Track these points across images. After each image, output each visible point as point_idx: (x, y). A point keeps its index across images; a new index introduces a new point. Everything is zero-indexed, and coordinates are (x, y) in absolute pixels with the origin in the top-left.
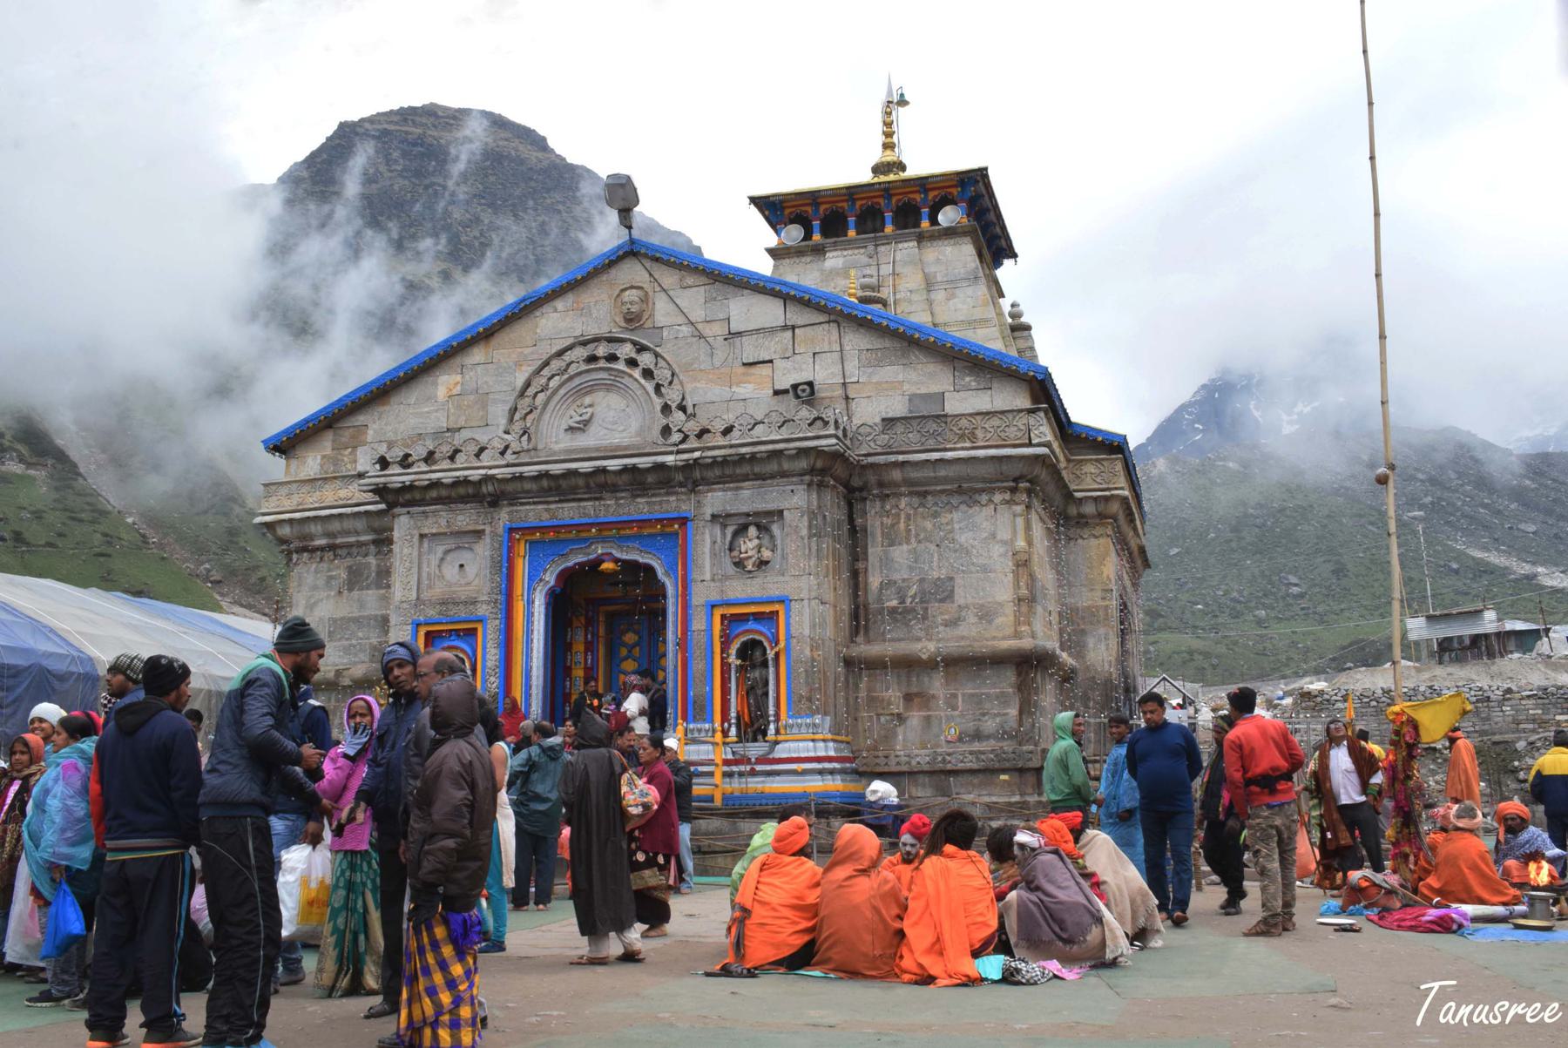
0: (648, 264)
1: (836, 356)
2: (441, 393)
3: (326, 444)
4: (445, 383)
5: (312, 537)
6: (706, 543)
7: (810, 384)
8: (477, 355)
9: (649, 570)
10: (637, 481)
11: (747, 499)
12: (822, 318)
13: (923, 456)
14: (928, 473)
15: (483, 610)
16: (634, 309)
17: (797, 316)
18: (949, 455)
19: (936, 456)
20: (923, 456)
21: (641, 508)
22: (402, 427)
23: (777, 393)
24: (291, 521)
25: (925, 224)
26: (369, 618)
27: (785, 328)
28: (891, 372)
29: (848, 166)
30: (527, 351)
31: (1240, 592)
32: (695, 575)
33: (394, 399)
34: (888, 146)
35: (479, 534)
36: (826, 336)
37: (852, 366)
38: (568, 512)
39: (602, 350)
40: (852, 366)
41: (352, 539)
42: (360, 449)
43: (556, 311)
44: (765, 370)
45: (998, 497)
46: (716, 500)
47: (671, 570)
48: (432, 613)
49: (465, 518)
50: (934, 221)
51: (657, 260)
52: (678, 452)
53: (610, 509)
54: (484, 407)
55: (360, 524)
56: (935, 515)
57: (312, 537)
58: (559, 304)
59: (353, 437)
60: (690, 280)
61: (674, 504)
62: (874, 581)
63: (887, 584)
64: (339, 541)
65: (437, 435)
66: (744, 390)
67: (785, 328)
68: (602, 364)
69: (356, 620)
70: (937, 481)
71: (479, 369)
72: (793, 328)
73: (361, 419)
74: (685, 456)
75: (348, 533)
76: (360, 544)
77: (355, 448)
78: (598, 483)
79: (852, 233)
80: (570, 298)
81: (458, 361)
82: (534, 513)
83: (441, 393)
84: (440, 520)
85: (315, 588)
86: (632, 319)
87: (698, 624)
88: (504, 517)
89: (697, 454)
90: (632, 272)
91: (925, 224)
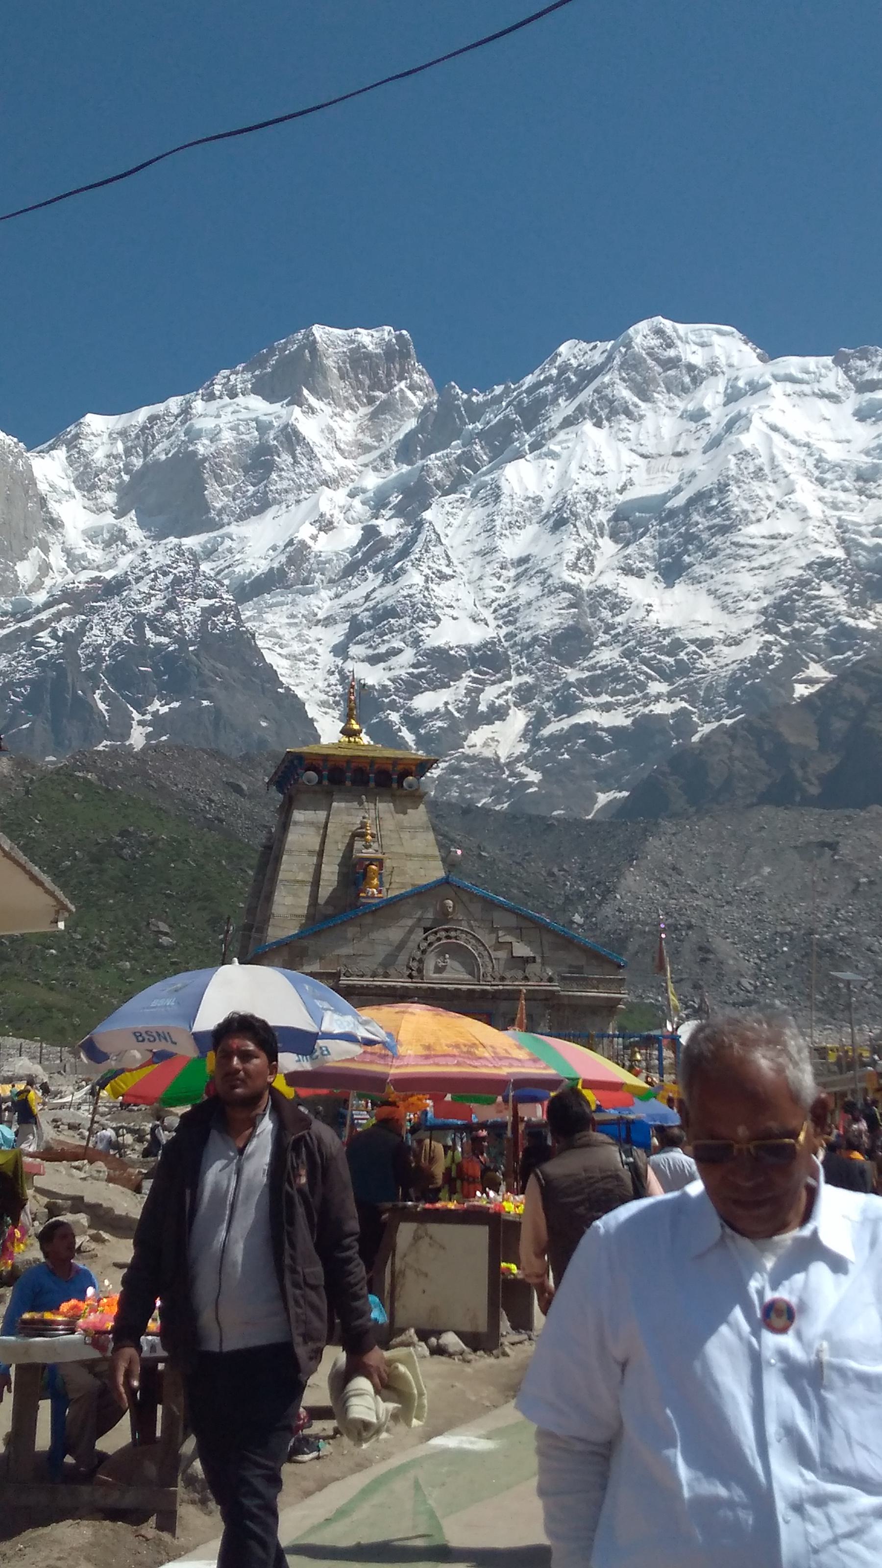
12: (532, 925)
13: (579, 994)
19: (584, 994)
20: (579, 994)
25: (395, 785)
27: (517, 928)
31: (101, 938)
43: (408, 903)
50: (400, 785)
52: (492, 985)
67: (517, 928)
72: (521, 929)
74: (495, 988)
79: (348, 783)
89: (501, 987)
91: (395, 785)
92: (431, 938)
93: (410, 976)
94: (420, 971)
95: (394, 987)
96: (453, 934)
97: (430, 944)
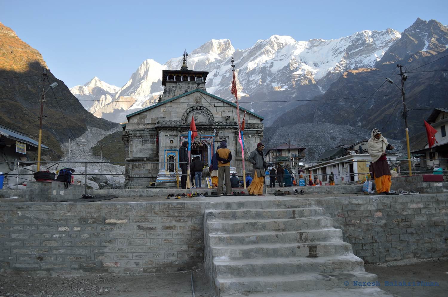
0: (200, 93)
1: (232, 112)
2: (162, 111)
3: (138, 116)
5: (136, 134)
7: (230, 116)
8: (169, 105)
12: (229, 106)
14: (247, 132)
16: (199, 101)
17: (226, 105)
18: (250, 129)
19: (248, 129)
22: (154, 116)
23: (222, 117)
24: (133, 131)
26: (148, 149)
29: (176, 66)
30: (179, 105)
32: (215, 145)
33: (152, 111)
34: (184, 63)
35: (176, 136)
36: (229, 109)
37: (234, 114)
39: (199, 108)
41: (145, 135)
42: (145, 119)
44: (221, 113)
45: (256, 136)
48: (168, 149)
49: (174, 133)
51: (202, 93)
54: (170, 114)
56: (247, 138)
57: (136, 134)
58: (184, 98)
59: (144, 117)
60: (208, 97)
62: (238, 148)
63: (239, 148)
64: (142, 135)
65: (161, 118)
66: (217, 116)
68: (199, 110)
69: (146, 149)
70: (248, 133)
71: (169, 107)
73: (145, 113)
75: (144, 134)
76: (146, 136)
77: (144, 119)
80: (186, 97)
81: (165, 105)
83: (162, 111)
84: (169, 133)
85: (137, 143)
86: (197, 102)
90: (197, 94)
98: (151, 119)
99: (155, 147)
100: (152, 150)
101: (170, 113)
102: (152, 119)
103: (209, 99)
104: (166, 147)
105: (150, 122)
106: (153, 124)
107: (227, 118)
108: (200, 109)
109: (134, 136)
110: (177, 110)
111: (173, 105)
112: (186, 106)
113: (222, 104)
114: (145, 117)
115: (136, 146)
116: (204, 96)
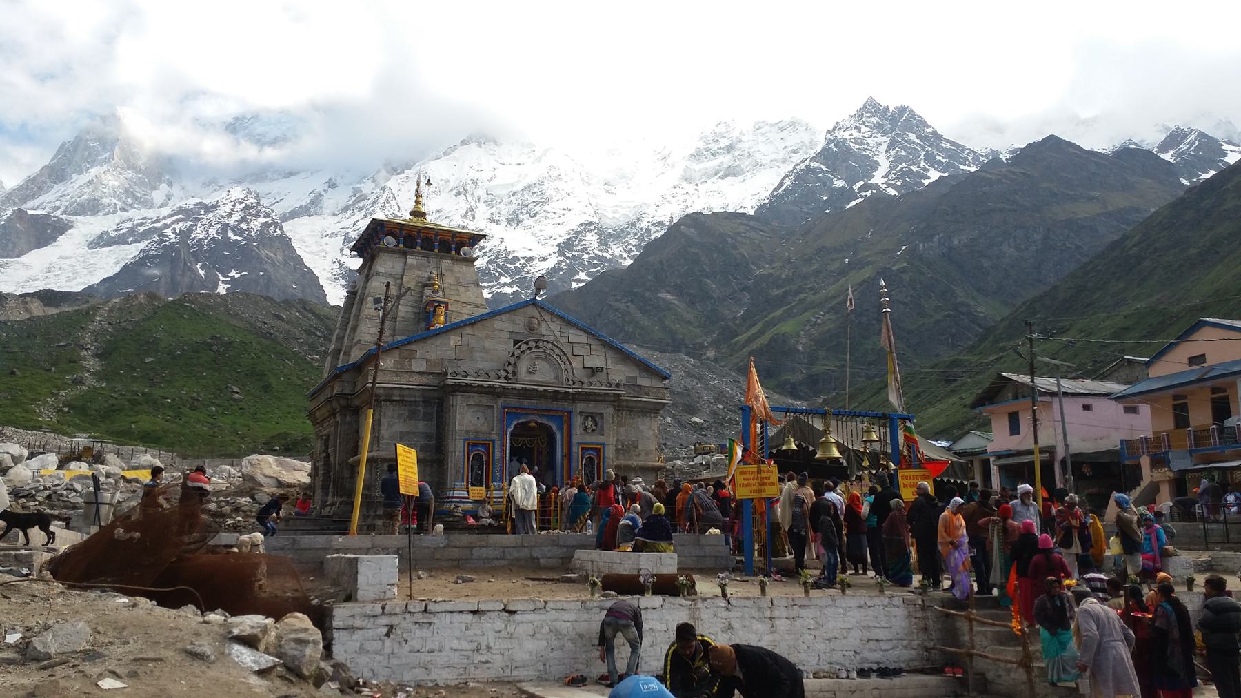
2: (452, 343)
3: (397, 352)
4: (454, 340)
5: (392, 395)
6: (577, 421)
8: (468, 330)
9: (549, 428)
10: (556, 396)
11: (591, 407)
15: (494, 437)
21: (555, 405)
28: (620, 367)
38: (526, 403)
40: (609, 362)
46: (580, 406)
47: (561, 429)
48: (471, 436)
49: (485, 400)
53: (543, 404)
55: (418, 394)
57: (392, 395)
58: (503, 317)
61: (566, 406)
65: (451, 360)
73: (413, 347)
78: (542, 395)
81: (459, 331)
82: (513, 402)
83: (452, 343)
84: (475, 399)
87: (575, 450)
88: (501, 401)
92: (524, 347)
93: (506, 378)
94: (514, 373)
95: (493, 387)
96: (541, 344)
97: (523, 352)
98: (428, 361)
99: (433, 430)
100: (428, 436)
101: (471, 350)
102: (428, 361)
103: (556, 327)
104: (467, 432)
105: (423, 369)
106: (429, 374)
107: (594, 371)
108: (537, 347)
109: (386, 401)
110: (488, 344)
111: (479, 331)
112: (507, 335)
113: (584, 339)
114: (412, 356)
115: (390, 426)
116: (547, 317)
